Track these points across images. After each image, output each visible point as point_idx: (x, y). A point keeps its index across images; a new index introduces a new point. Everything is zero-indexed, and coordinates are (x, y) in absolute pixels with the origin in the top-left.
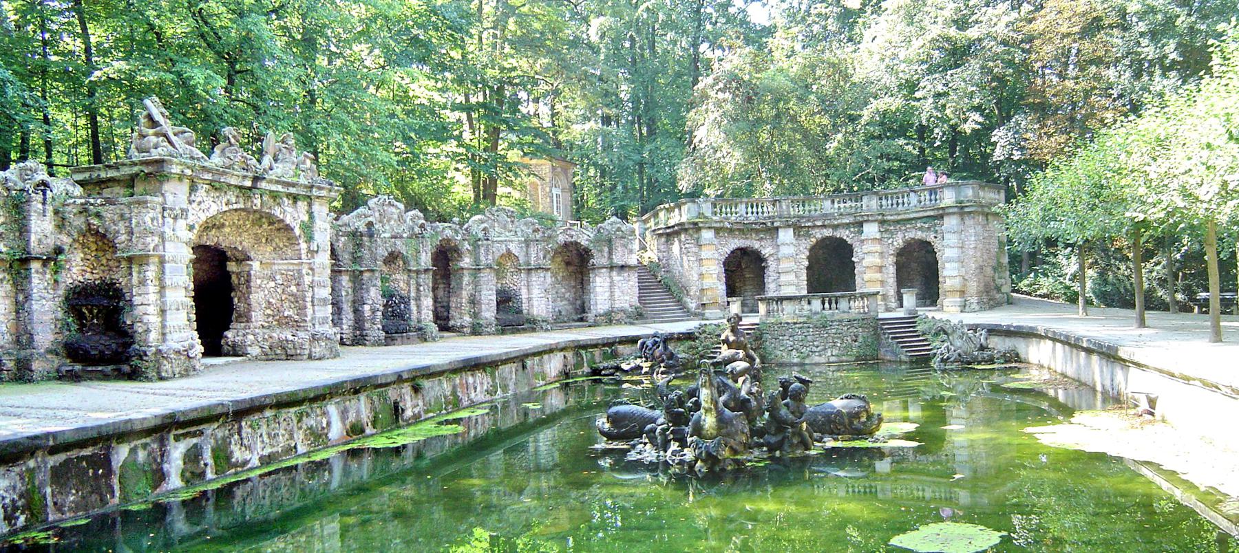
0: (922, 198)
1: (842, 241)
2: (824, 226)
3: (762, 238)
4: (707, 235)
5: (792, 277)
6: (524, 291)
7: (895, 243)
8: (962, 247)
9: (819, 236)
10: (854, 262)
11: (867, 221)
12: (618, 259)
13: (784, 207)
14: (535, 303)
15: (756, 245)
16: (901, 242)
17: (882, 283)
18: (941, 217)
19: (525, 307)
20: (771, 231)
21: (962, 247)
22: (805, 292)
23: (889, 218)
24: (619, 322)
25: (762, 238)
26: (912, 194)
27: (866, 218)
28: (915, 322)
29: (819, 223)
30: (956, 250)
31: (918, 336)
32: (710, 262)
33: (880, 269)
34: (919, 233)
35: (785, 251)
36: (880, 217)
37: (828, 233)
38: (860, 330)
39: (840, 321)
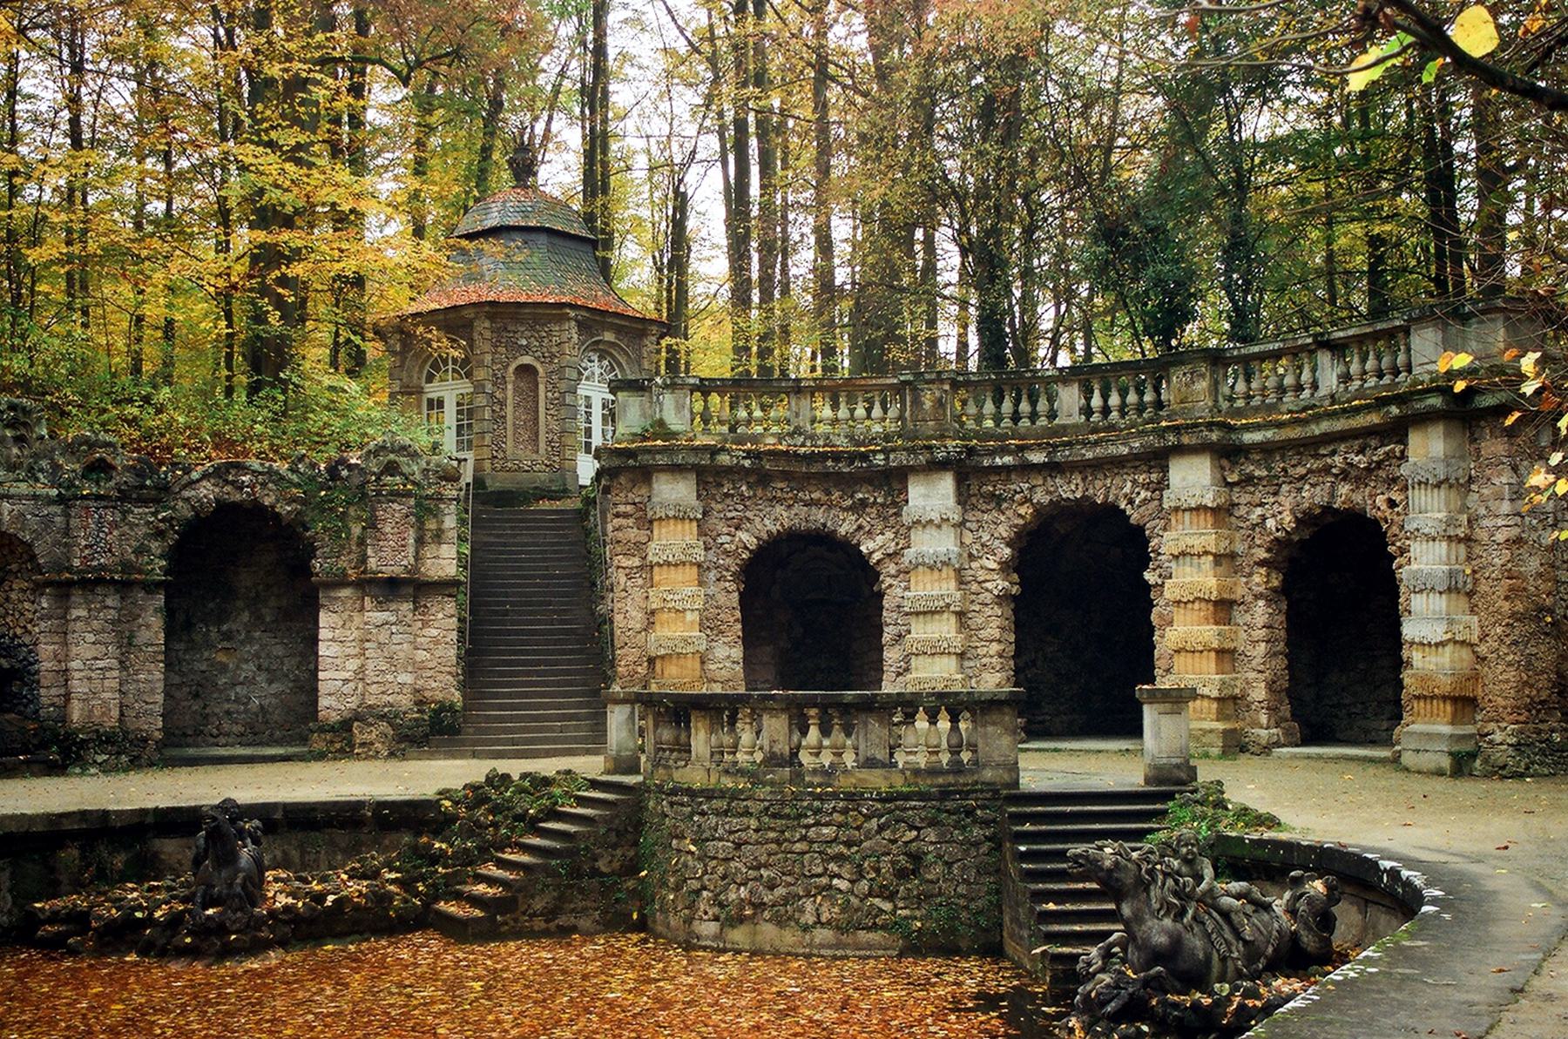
0: (1355, 368)
1: (1112, 513)
2: (1052, 469)
3: (863, 504)
4: (675, 491)
5: (944, 629)
6: (46, 650)
7: (1271, 523)
8: (1468, 540)
9: (1040, 497)
10: (1147, 587)
11: (1181, 450)
12: (387, 559)
13: (928, 405)
14: (78, 687)
15: (846, 526)
16: (1287, 518)
17: (1226, 656)
18: (1397, 431)
19: (48, 695)
20: (894, 481)
21: (1468, 540)
22: (993, 680)
23: (1249, 437)
24: (368, 753)
25: (863, 504)
26: (1324, 358)
27: (1172, 439)
28: (1164, 813)
29: (1037, 457)
30: (1442, 548)
31: (1061, 876)
32: (676, 575)
33: (1223, 608)
34: (1344, 489)
35: (935, 544)
36: (1214, 436)
37: (1070, 489)
38: (931, 835)
39: (850, 797)
